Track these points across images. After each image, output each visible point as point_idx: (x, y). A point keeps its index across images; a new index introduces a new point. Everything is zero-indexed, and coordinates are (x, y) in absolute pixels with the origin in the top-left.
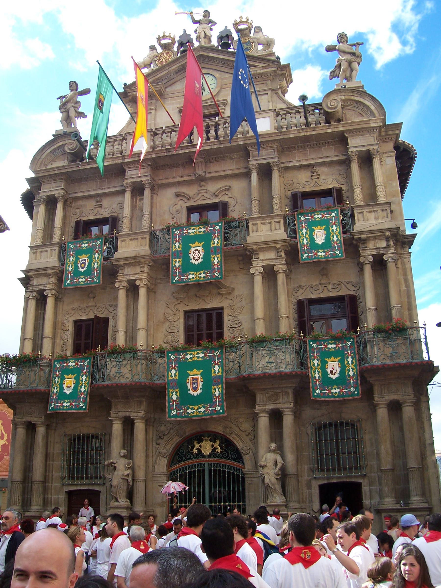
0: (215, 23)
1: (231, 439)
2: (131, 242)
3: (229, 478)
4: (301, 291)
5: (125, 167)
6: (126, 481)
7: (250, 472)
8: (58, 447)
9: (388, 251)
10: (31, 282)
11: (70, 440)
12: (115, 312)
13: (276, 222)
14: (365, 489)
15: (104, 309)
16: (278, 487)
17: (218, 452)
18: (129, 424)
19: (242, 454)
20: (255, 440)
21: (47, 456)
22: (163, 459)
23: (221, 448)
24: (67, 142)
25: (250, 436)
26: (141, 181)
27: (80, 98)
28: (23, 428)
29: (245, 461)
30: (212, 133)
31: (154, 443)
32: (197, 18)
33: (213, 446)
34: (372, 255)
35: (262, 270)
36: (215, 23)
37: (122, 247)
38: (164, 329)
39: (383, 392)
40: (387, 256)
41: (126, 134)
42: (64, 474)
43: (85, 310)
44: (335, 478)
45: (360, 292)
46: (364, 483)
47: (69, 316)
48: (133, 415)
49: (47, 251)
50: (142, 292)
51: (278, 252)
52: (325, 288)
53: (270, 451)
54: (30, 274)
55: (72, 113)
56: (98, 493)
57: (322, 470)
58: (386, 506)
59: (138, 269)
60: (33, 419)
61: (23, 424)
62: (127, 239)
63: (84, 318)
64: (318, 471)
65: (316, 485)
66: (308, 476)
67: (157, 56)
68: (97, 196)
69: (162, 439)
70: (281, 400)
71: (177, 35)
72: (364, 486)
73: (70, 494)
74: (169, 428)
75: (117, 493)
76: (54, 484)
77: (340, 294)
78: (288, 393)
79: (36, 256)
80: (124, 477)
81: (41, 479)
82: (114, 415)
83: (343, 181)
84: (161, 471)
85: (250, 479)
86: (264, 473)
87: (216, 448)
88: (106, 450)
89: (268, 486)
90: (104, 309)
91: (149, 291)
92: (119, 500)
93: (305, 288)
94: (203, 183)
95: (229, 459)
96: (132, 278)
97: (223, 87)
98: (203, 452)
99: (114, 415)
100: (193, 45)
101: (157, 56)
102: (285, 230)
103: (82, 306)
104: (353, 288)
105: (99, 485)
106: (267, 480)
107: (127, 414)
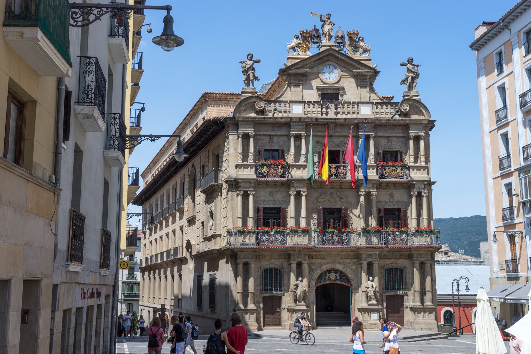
0: (334, 24)
16: (373, 297)
24: (255, 100)
30: (339, 110)
32: (324, 19)
36: (334, 24)
50: (303, 198)
55: (251, 78)
63: (268, 206)
68: (271, 135)
71: (310, 28)
73: (263, 297)
83: (403, 147)
96: (299, 190)
100: (320, 39)
102: (377, 174)
106: (369, 294)
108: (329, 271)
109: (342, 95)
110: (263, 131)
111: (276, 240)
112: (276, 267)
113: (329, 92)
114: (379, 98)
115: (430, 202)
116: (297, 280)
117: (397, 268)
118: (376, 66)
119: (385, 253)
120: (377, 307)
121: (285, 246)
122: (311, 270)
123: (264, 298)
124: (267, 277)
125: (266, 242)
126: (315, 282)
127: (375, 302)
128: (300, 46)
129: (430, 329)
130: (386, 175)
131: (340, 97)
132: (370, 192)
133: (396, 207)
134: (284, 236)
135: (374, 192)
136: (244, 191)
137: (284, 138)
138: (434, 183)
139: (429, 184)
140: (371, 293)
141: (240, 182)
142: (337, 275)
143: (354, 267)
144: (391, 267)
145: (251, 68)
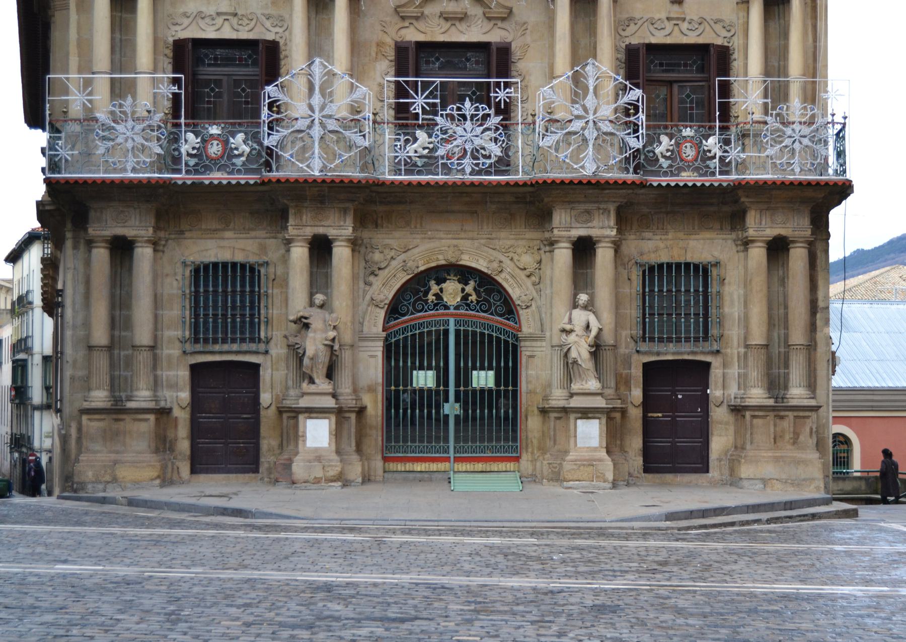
1: (500, 280)
3: (474, 343)
4: (632, 28)
6: (329, 349)
7: (532, 338)
8: (176, 285)
11: (197, 271)
12: (277, 29)
14: (716, 373)
17: (472, 302)
18: (321, 249)
19: (518, 308)
20: (541, 285)
21: (157, 302)
22: (378, 310)
23: (478, 294)
25: (533, 278)
28: (106, 248)
29: (522, 318)
31: (362, 284)
33: (463, 290)
38: (378, 74)
39: (763, 222)
42: (187, 333)
43: (213, 19)
44: (670, 353)
45: (736, 43)
46: (716, 363)
47: (178, 28)
48: (331, 232)
52: (676, 28)
53: (575, 306)
56: (256, 367)
57: (652, 339)
58: (753, 400)
60: (128, 232)
61: (106, 241)
63: (211, 34)
64: (644, 341)
65: (638, 361)
66: (626, 348)
69: (376, 275)
70: (595, 223)
72: (716, 368)
74: (389, 257)
75: (314, 369)
76: (166, 352)
77: (701, 40)
78: (609, 212)
80: (327, 342)
81: (151, 344)
82: (295, 232)
84: (374, 330)
85: (529, 349)
86: (569, 341)
88: (270, 291)
89: (575, 362)
92: (317, 381)
93: (640, 23)
95: (492, 314)
98: (445, 300)
99: (295, 232)
103: (204, 9)
104: (724, 33)
105: (257, 353)
106: (573, 354)
107: (321, 231)
108: (440, 273)
111: (231, 157)
112: (239, 258)
116: (312, 304)
117: (687, 265)
119: (645, 210)
120: (600, 402)
121: (267, 175)
123: (195, 369)
125: (192, 162)
126: (382, 314)
127: (593, 384)
129: (797, 483)
133: (691, 39)
140: (581, 350)
142: (469, 289)
143: (527, 260)
144: (664, 259)
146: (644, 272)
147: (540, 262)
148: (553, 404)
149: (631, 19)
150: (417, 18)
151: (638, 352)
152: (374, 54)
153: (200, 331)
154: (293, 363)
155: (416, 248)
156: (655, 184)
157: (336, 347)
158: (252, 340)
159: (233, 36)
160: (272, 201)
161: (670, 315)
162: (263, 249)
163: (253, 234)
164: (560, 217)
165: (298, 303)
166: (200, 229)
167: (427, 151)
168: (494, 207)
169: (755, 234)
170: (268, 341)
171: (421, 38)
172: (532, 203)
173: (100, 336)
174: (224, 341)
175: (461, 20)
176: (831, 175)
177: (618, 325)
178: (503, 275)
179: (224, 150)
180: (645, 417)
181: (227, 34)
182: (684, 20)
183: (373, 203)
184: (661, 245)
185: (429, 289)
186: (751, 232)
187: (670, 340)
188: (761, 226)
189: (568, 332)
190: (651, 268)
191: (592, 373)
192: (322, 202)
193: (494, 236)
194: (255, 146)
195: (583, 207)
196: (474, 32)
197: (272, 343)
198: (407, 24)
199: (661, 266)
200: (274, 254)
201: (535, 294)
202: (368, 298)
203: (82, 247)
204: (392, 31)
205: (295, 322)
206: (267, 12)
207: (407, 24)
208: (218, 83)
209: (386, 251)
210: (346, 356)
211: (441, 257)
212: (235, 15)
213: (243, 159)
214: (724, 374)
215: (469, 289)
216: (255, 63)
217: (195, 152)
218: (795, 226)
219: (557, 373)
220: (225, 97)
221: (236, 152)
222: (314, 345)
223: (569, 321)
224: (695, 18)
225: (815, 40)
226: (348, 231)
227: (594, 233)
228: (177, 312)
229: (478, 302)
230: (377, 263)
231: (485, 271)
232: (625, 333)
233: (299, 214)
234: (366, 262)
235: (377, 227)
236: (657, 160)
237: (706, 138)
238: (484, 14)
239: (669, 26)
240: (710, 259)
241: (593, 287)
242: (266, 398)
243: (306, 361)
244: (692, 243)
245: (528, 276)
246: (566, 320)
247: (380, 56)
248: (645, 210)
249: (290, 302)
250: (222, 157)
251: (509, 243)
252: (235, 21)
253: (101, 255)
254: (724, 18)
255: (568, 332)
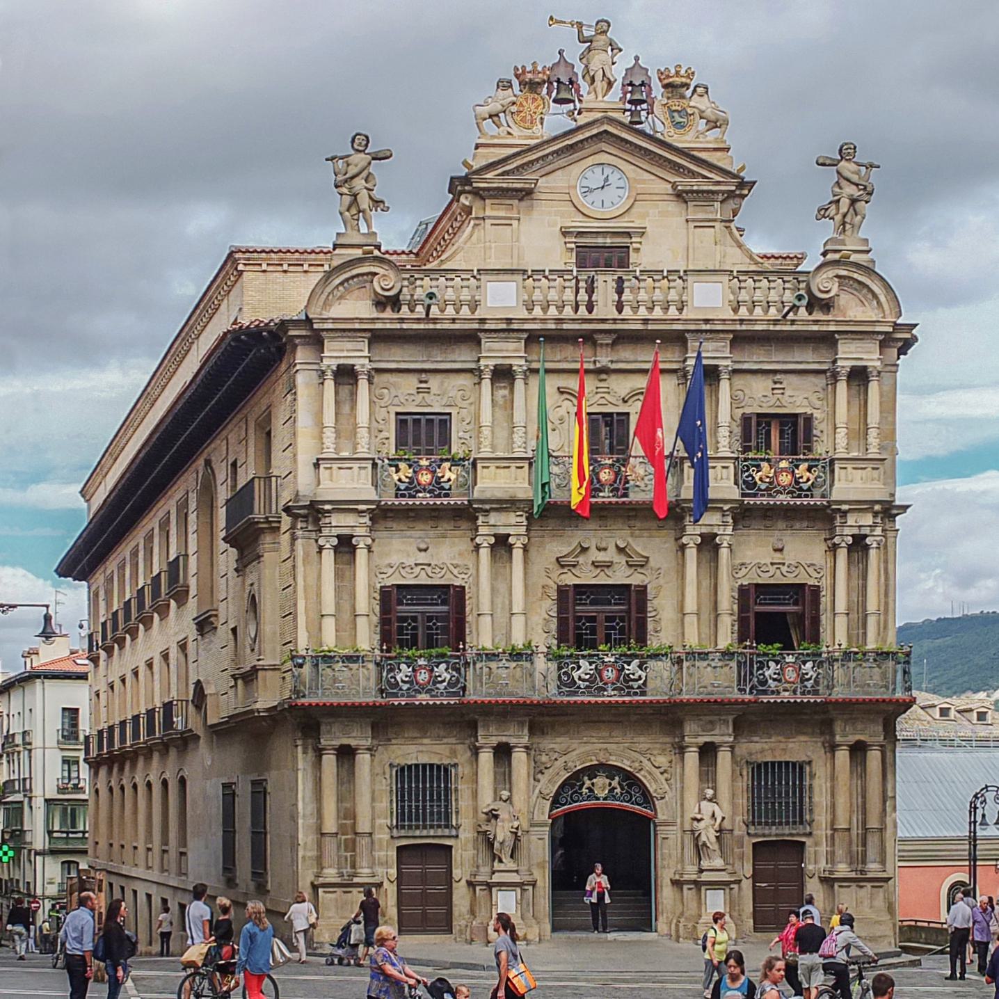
2: (498, 470)
4: (744, 571)
5: (481, 335)
7: (665, 824)
9: (873, 531)
10: (327, 520)
11: (402, 769)
12: (463, 576)
13: (724, 467)
15: (444, 571)
16: (716, 847)
18: (503, 753)
23: (622, 788)
25: (666, 775)
26: (511, 365)
27: (375, 167)
29: (657, 807)
31: (532, 779)
33: (610, 784)
34: (852, 536)
35: (699, 540)
37: (483, 478)
40: (872, 538)
41: (478, 270)
45: (825, 583)
48: (513, 741)
49: (351, 468)
50: (518, 554)
51: (723, 515)
52: (778, 571)
54: (327, 507)
57: (760, 823)
59: (512, 518)
62: (492, 465)
67: (514, 103)
70: (717, 731)
73: (399, 849)
77: (797, 581)
79: (331, 475)
87: (615, 788)
89: (704, 844)
90: (444, 571)
91: (525, 549)
94: (604, 376)
96: (502, 531)
97: (639, 197)
101: (514, 103)
102: (736, 483)
105: (449, 837)
106: (703, 838)
107: (504, 739)
108: (591, 771)
109: (637, 250)
110: (397, 357)
111: (435, 683)
112: (436, 761)
113: (600, 241)
114: (751, 258)
115: (891, 567)
116: (497, 797)
117: (787, 763)
118: (743, 168)
119: (754, 718)
122: (538, 770)
123: (400, 849)
124: (410, 787)
125: (405, 687)
126: (548, 803)
127: (718, 862)
128: (514, 108)
130: (763, 487)
131: (633, 257)
132: (716, 535)
134: (458, 671)
135: (726, 535)
136: (338, 536)
137: (465, 381)
138: (905, 508)
139: (888, 511)
140: (709, 836)
141: (328, 511)
142: (615, 783)
143: (662, 760)
144: (769, 759)
145: (364, 174)
146: (753, 769)
147: (670, 762)
148: (686, 877)
149: (743, 564)
150: (574, 566)
151: (748, 834)
152: (540, 595)
153: (404, 818)
154: (482, 847)
155: (574, 751)
156: (765, 701)
157: (519, 834)
158: (447, 827)
159: (429, 582)
160: (464, 719)
161: (773, 804)
162: (454, 753)
163: (445, 740)
164: (690, 727)
165: (486, 799)
166: (404, 737)
167: (588, 676)
168: (635, 718)
169: (842, 739)
170: (458, 828)
171: (578, 582)
172: (668, 718)
173: (330, 825)
174: (425, 827)
175: (608, 567)
176: (899, 695)
177: (734, 814)
178: (642, 772)
179: (431, 677)
180: (754, 886)
181: (423, 580)
182: (784, 564)
183: (542, 718)
184: (766, 747)
185: (584, 784)
186: (838, 738)
187: (774, 824)
188: (846, 735)
189: (699, 820)
190: (759, 766)
191: (718, 852)
192: (505, 717)
193: (635, 740)
194: (454, 673)
195: (709, 718)
196: (620, 576)
197: (461, 830)
198: (566, 570)
199: (766, 763)
200: (463, 756)
201: (667, 787)
202: (537, 791)
203: (311, 753)
204: (554, 575)
205: (486, 814)
206: (454, 562)
207: (566, 570)
208: (414, 619)
209: (551, 754)
210: (524, 839)
211: (593, 758)
212: (429, 565)
213: (445, 684)
214: (815, 852)
215: (615, 783)
216: (444, 603)
217: (407, 679)
218: (872, 733)
219: (689, 851)
220: (420, 629)
221: (439, 679)
222: (502, 832)
223: (697, 807)
224: (793, 563)
225: (887, 579)
226: (525, 740)
227: (717, 739)
228: (386, 804)
229: (622, 794)
230: (544, 763)
231: (629, 769)
232: (739, 819)
233: (486, 727)
234: (535, 763)
235: (543, 733)
236: (767, 681)
237: (804, 663)
238: (627, 562)
239: (772, 569)
240: (807, 759)
241: (714, 781)
242: (457, 873)
243: (496, 845)
244: (791, 745)
245: (662, 773)
246: (697, 810)
247: (545, 596)
248: (754, 718)
249: (479, 796)
250: (429, 683)
251: (647, 746)
252: (429, 569)
253: (329, 760)
254: (814, 562)
255: (699, 820)
